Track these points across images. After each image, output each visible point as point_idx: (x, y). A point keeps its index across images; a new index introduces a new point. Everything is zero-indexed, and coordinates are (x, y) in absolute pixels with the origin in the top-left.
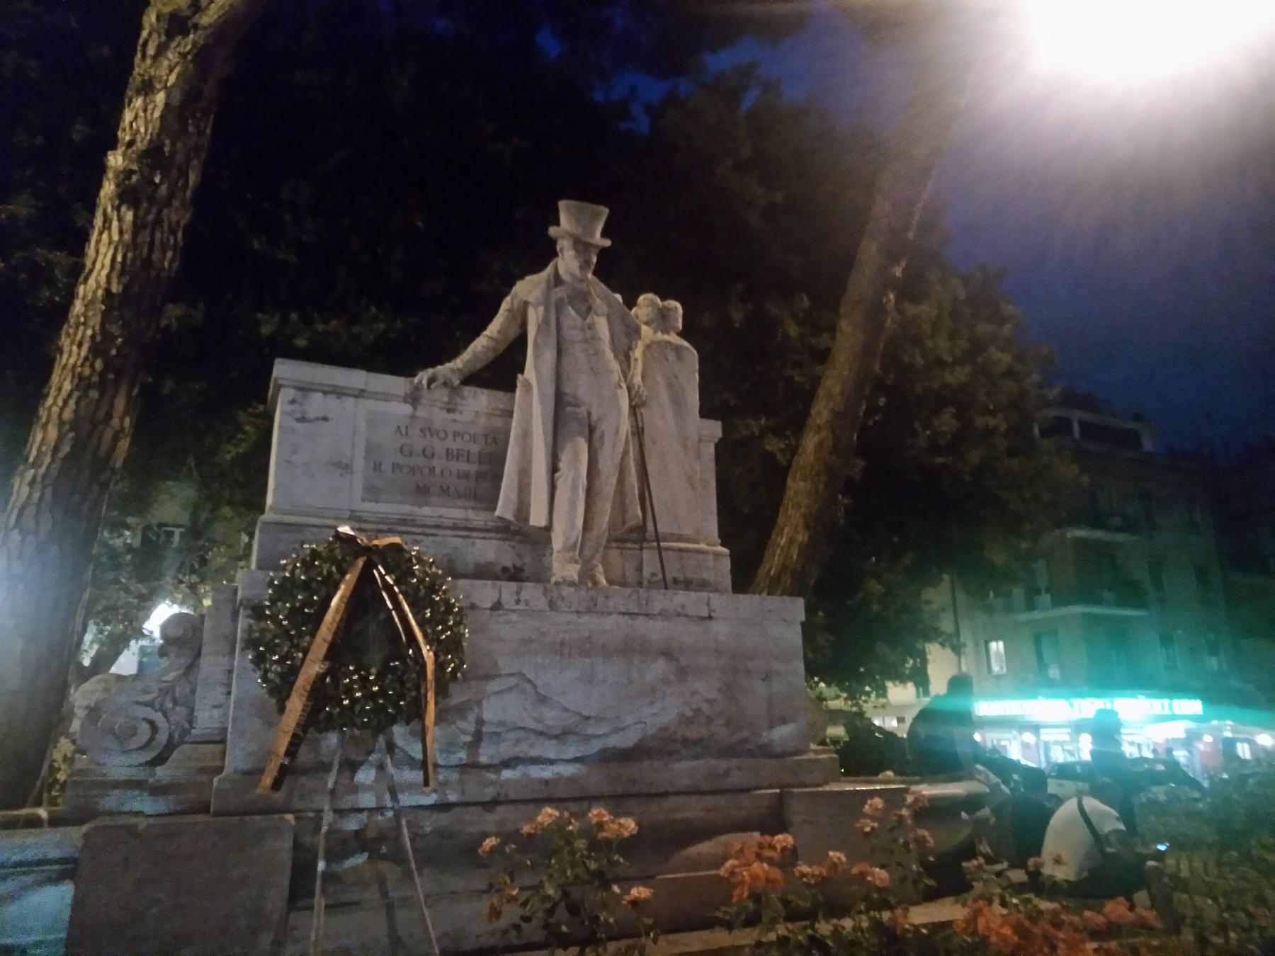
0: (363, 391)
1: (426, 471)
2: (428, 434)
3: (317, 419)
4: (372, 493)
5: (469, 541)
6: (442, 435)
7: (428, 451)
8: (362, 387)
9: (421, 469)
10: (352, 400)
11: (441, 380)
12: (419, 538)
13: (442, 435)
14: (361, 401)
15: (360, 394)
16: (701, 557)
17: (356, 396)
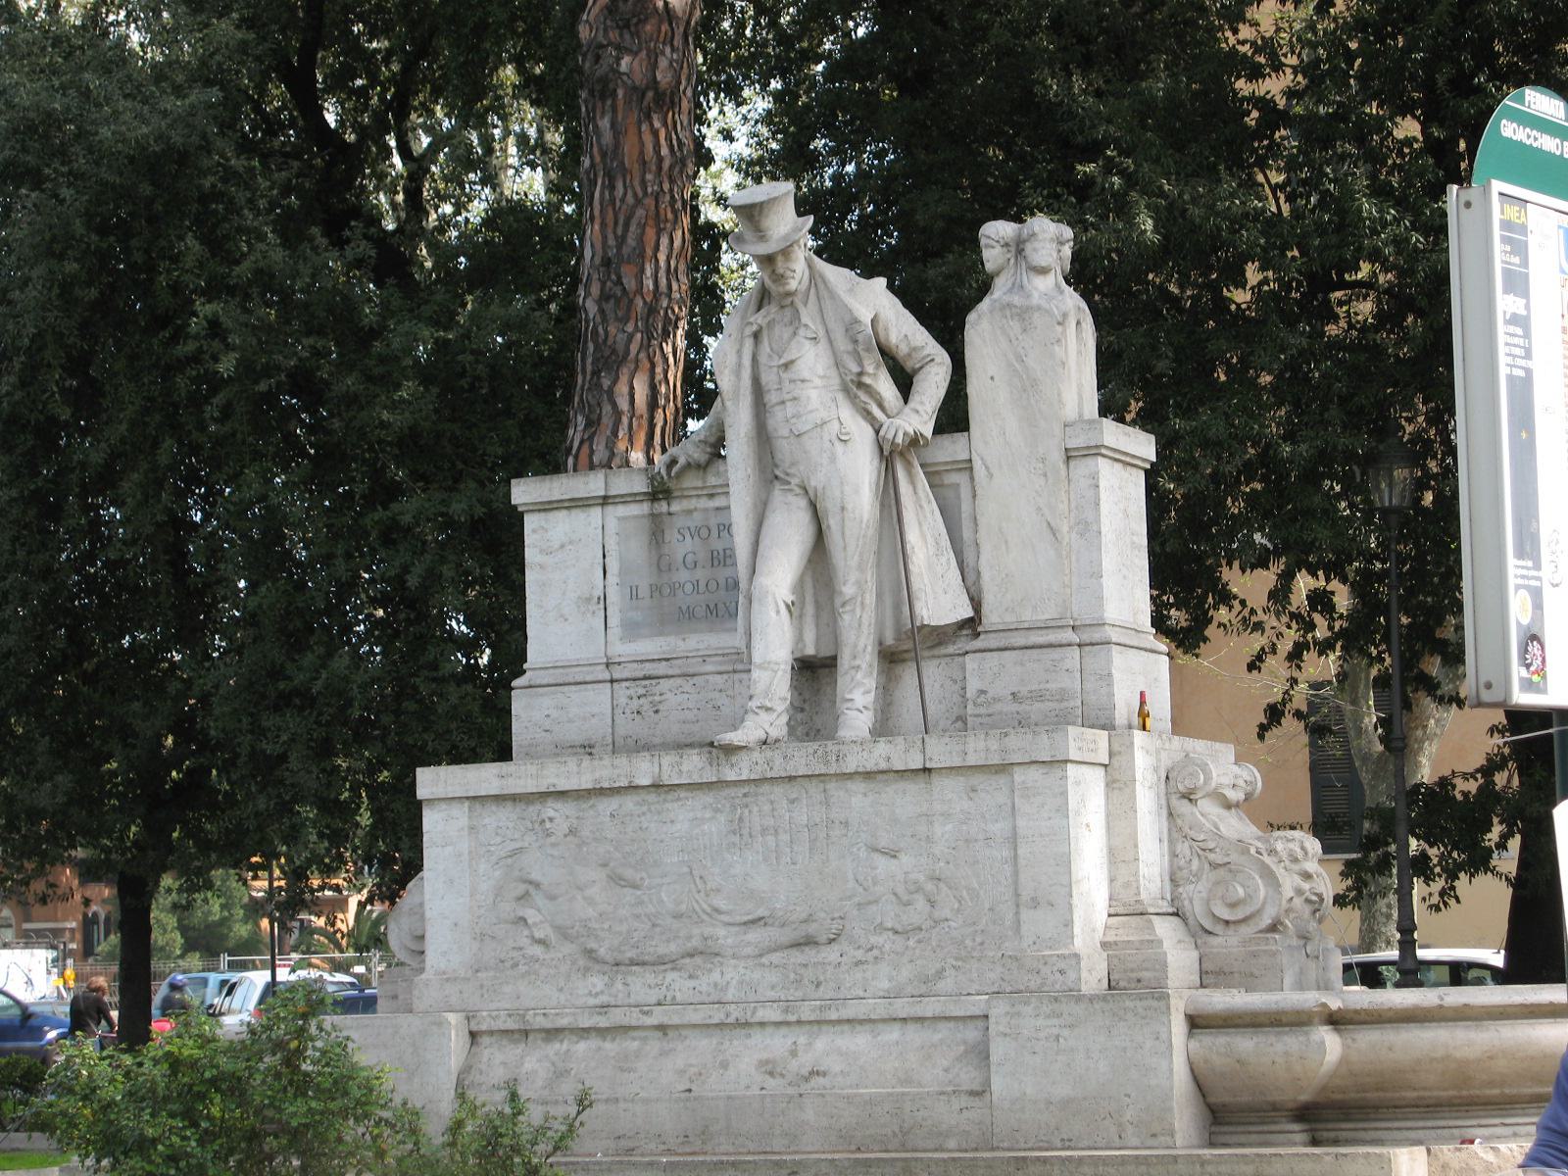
0: (605, 498)
1: (689, 588)
2: (688, 536)
3: (562, 546)
4: (631, 631)
5: (737, 676)
6: (704, 533)
7: (690, 558)
8: (602, 493)
9: (682, 586)
10: (598, 510)
11: (682, 461)
12: (679, 681)
13: (704, 533)
14: (610, 509)
15: (605, 501)
16: (1056, 654)
17: (603, 505)
